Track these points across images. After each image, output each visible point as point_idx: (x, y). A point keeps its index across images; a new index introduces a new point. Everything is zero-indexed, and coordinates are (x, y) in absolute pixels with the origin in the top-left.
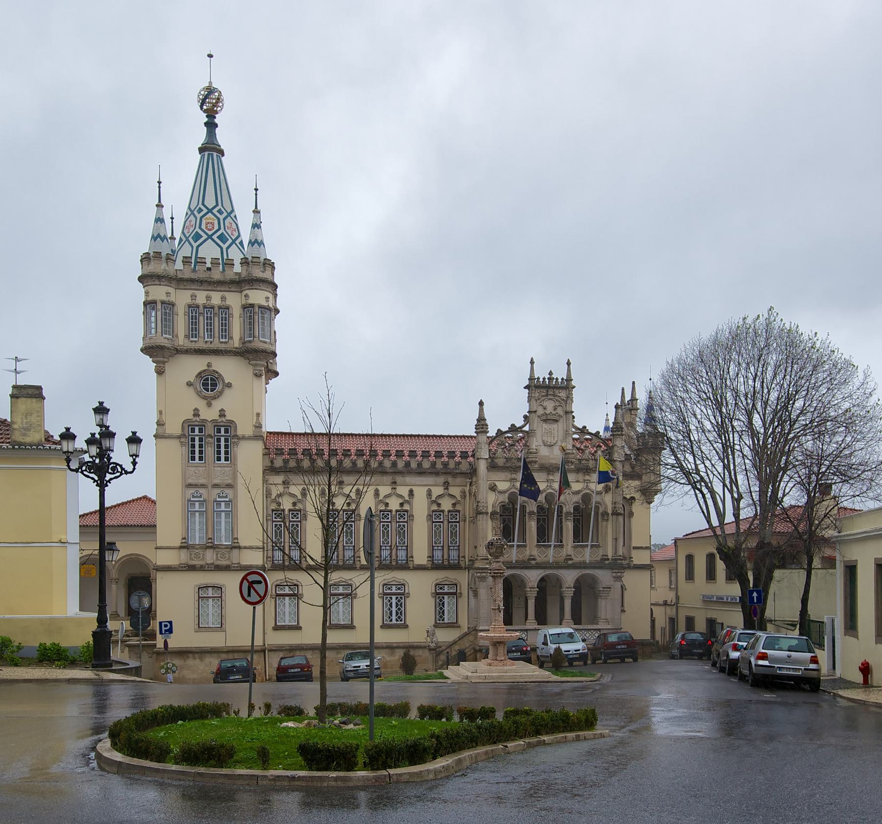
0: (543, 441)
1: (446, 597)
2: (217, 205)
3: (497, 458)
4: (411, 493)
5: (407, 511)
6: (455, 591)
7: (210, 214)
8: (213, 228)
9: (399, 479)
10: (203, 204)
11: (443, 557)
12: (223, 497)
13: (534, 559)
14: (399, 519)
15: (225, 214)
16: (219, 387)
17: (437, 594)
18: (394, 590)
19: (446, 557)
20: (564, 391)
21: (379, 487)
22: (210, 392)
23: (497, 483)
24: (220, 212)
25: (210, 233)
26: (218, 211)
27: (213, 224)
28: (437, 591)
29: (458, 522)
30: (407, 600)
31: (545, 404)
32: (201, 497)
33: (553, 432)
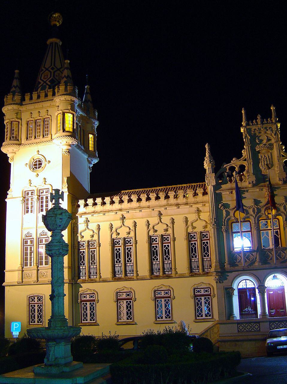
1: (203, 298)
2: (51, 65)
6: (210, 293)
7: (47, 71)
8: (47, 77)
10: (44, 67)
12: (44, 235)
15: (56, 69)
16: (42, 166)
22: (38, 169)
24: (53, 69)
25: (45, 80)
26: (51, 69)
27: (47, 75)
28: (196, 294)
29: (209, 240)
30: (173, 301)
32: (31, 236)
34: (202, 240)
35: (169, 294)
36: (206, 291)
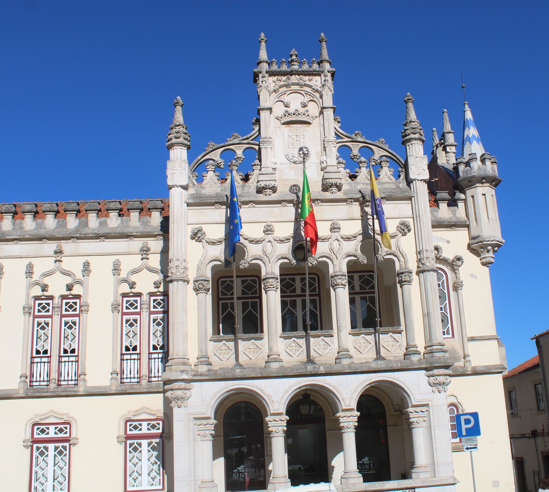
0: (287, 156)
1: (145, 443)
3: (204, 188)
4: (86, 269)
5: (78, 297)
9: (67, 246)
11: (139, 371)
13: (276, 360)
14: (66, 310)
17: (129, 437)
18: (52, 433)
19: (145, 372)
20: (318, 78)
21: (33, 261)
23: (205, 228)
31: (286, 98)
33: (302, 141)
34: (151, 313)
35: (66, 433)
36: (154, 427)
